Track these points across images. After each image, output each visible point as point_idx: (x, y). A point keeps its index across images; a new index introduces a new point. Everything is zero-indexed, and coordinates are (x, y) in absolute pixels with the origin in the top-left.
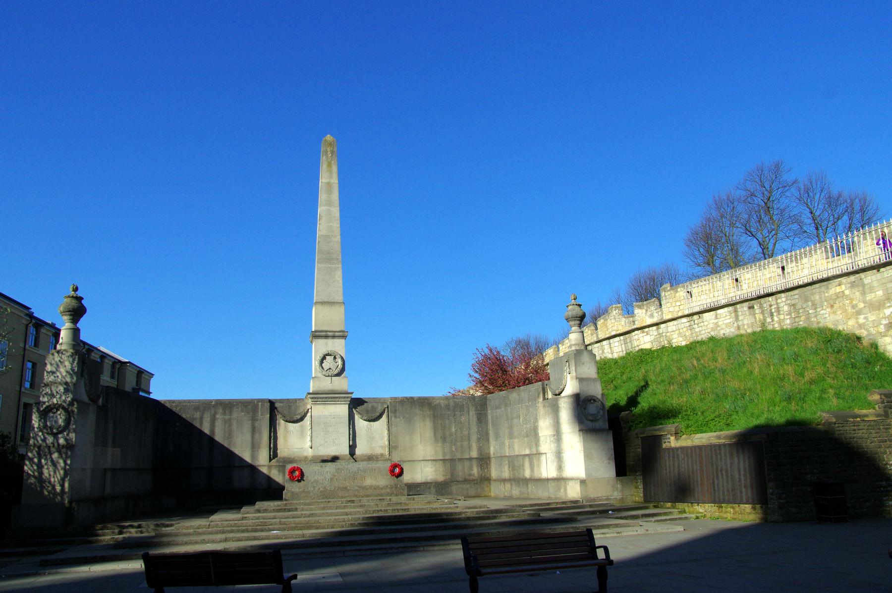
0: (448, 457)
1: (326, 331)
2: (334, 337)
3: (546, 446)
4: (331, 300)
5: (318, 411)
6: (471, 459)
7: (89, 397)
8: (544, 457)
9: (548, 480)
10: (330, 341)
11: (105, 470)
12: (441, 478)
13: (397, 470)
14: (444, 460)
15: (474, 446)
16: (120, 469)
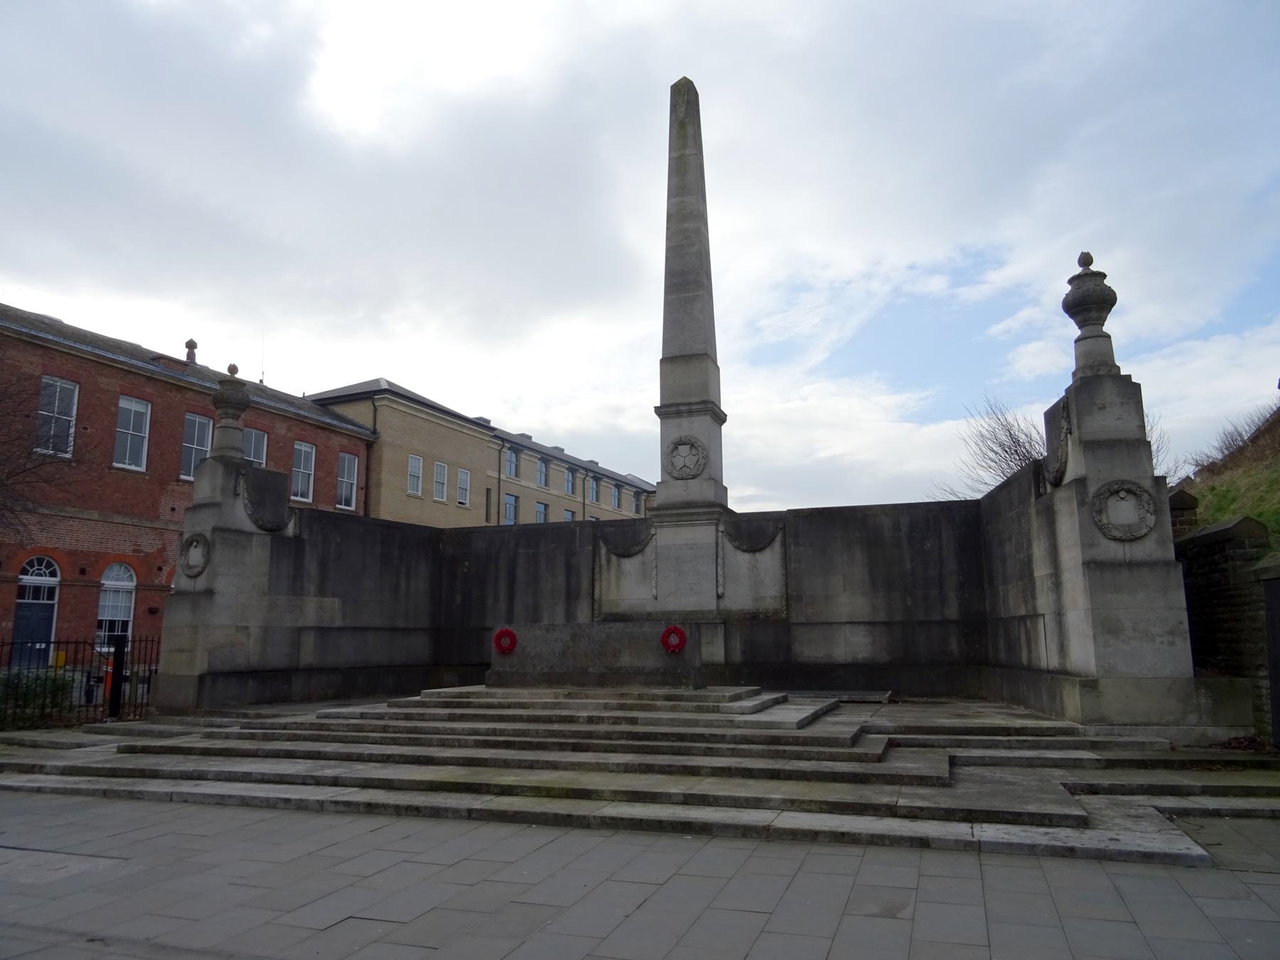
0: (898, 618)
1: (678, 405)
2: (690, 413)
3: (1044, 602)
4: (687, 352)
5: (666, 537)
6: (945, 622)
7: (255, 522)
8: (1041, 620)
9: (1049, 671)
10: (685, 422)
11: (300, 630)
12: (884, 657)
13: (674, 640)
15: (953, 596)
16: (340, 629)
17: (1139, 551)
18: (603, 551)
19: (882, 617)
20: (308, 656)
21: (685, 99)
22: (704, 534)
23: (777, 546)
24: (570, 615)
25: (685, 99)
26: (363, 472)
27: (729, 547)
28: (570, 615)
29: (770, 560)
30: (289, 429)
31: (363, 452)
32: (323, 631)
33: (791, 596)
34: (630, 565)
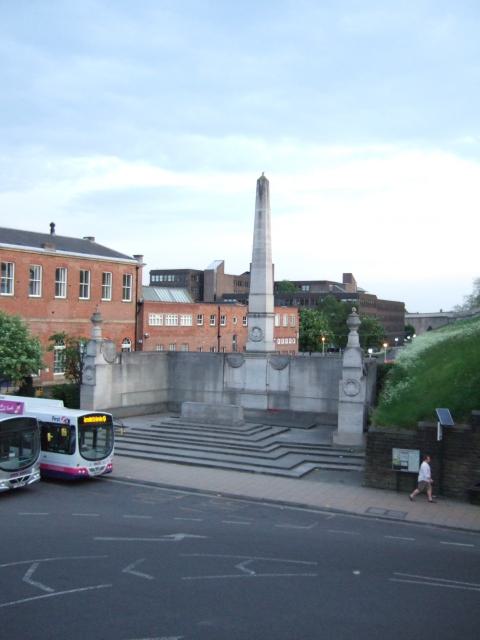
2: (259, 316)
14: (323, 399)
17: (355, 399)
18: (227, 365)
19: (321, 397)
20: (125, 403)
21: (262, 186)
22: (262, 363)
23: (287, 368)
24: (215, 387)
25: (262, 186)
26: (135, 283)
27: (270, 368)
28: (215, 387)
29: (285, 372)
30: (100, 267)
31: (134, 272)
32: (129, 393)
33: (291, 388)
34: (237, 372)
